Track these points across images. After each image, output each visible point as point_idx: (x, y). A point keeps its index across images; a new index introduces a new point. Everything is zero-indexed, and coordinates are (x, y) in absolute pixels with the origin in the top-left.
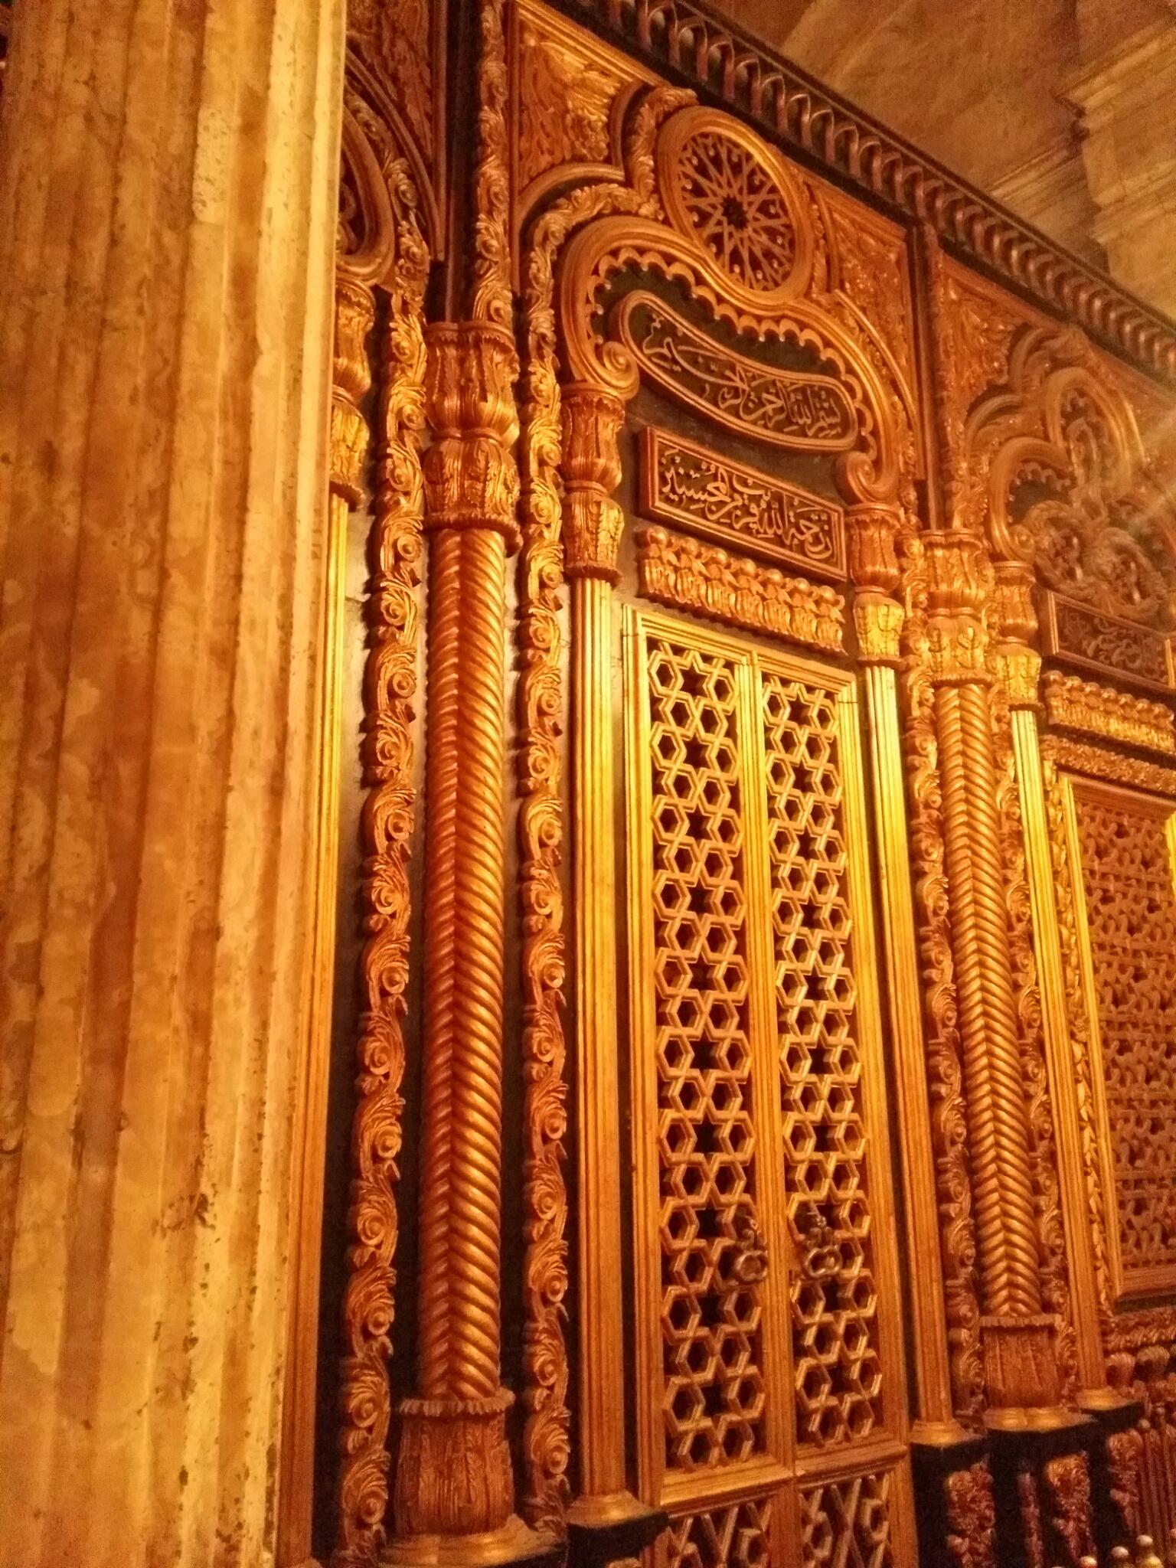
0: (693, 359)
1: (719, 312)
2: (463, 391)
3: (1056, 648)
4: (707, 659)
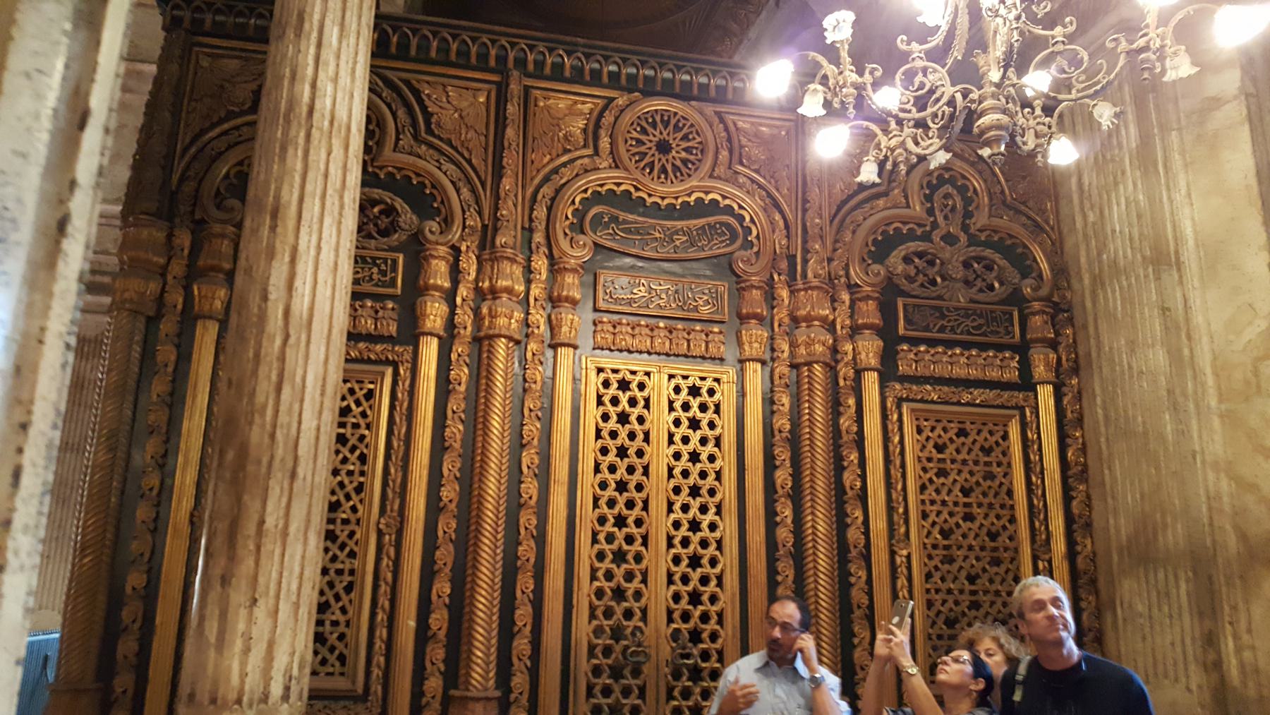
1: (649, 200)
2: (491, 279)
3: (901, 331)
4: (633, 373)
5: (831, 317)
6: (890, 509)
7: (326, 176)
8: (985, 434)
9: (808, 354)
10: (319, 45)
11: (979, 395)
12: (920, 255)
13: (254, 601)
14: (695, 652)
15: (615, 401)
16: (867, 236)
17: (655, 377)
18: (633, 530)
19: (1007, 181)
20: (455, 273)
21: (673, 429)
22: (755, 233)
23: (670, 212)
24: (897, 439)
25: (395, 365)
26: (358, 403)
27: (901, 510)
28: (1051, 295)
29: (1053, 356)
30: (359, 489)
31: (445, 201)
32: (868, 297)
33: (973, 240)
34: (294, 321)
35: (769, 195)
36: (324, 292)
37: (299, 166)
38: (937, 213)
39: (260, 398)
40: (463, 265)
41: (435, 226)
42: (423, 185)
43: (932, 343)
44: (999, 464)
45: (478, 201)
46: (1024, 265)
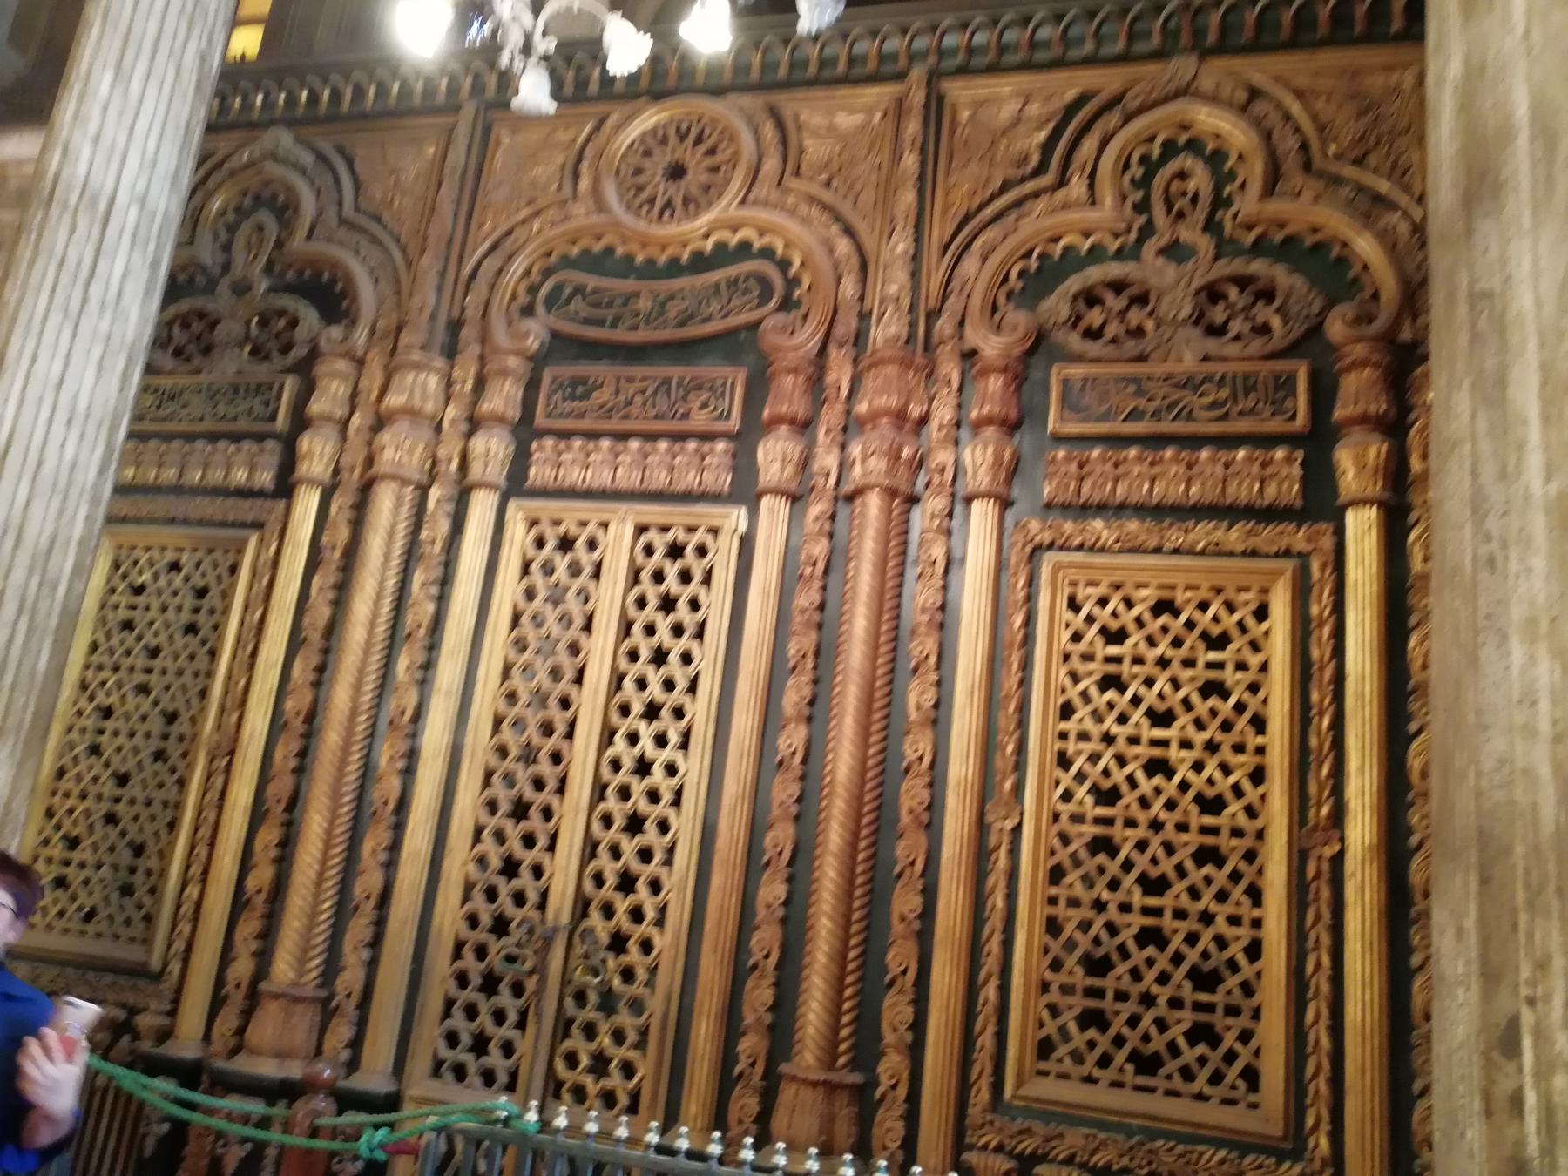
0: (597, 305)
5: (915, 410)
9: (864, 475)
11: (1203, 533)
12: (1118, 287)
17: (612, 528)
19: (1321, 129)
22: (806, 283)
23: (675, 268)
24: (1018, 621)
27: (1010, 748)
35: (838, 218)
37: (28, 254)
42: (333, 281)
44: (1241, 666)
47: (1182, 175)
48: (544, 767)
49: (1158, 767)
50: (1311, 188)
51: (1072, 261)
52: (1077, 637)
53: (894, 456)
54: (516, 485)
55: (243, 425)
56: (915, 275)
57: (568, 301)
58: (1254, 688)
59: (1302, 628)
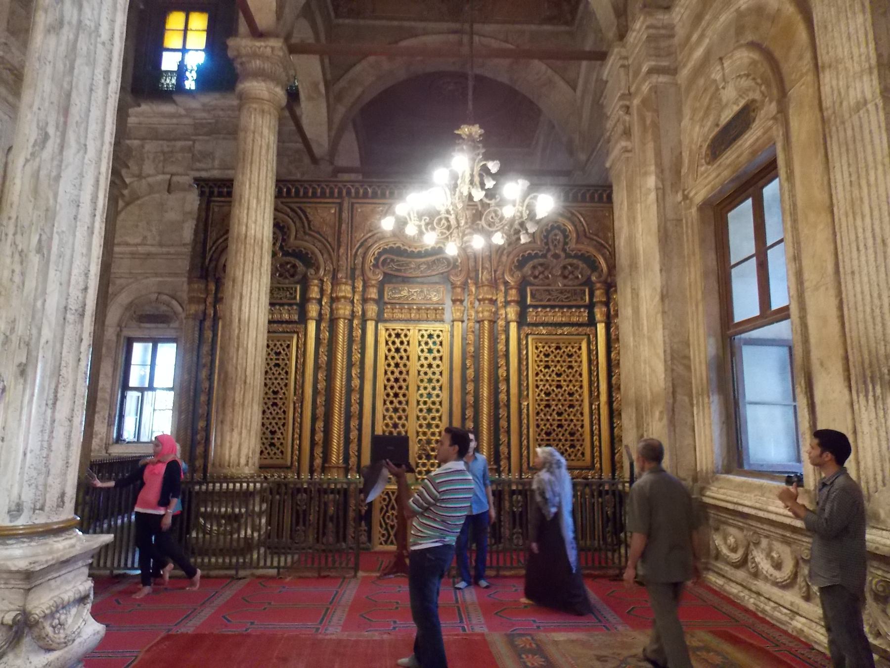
0: (398, 265)
1: (409, 250)
3: (529, 302)
4: (402, 330)
5: (494, 298)
6: (520, 384)
7: (253, 262)
8: (570, 348)
10: (248, 209)
11: (566, 330)
12: (541, 265)
13: (233, 430)
14: (428, 448)
15: (394, 343)
16: (513, 259)
17: (411, 331)
18: (401, 398)
20: (322, 292)
21: (420, 354)
25: (298, 333)
26: (284, 350)
28: (607, 279)
29: (604, 309)
30: (286, 385)
31: (317, 260)
32: (511, 288)
33: (568, 256)
34: (242, 323)
36: (254, 310)
37: (242, 259)
38: (550, 244)
39: (231, 354)
40: (325, 288)
41: (313, 271)
42: (307, 254)
43: (544, 307)
44: (576, 362)
45: (331, 259)
46: (593, 265)
47: (556, 235)
48: (401, 398)
49: (559, 386)
50: (586, 241)
51: (530, 257)
52: (538, 356)
53: (490, 311)
54: (379, 319)
55: (284, 301)
56: (490, 261)
57: (389, 264)
58: (579, 366)
59: (589, 351)
